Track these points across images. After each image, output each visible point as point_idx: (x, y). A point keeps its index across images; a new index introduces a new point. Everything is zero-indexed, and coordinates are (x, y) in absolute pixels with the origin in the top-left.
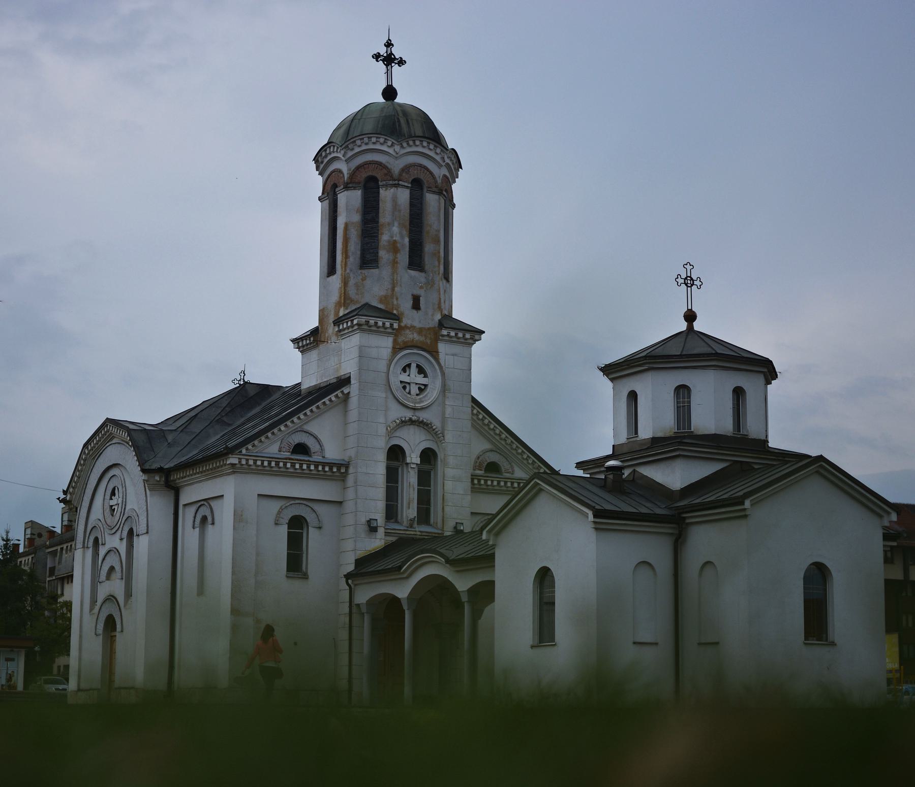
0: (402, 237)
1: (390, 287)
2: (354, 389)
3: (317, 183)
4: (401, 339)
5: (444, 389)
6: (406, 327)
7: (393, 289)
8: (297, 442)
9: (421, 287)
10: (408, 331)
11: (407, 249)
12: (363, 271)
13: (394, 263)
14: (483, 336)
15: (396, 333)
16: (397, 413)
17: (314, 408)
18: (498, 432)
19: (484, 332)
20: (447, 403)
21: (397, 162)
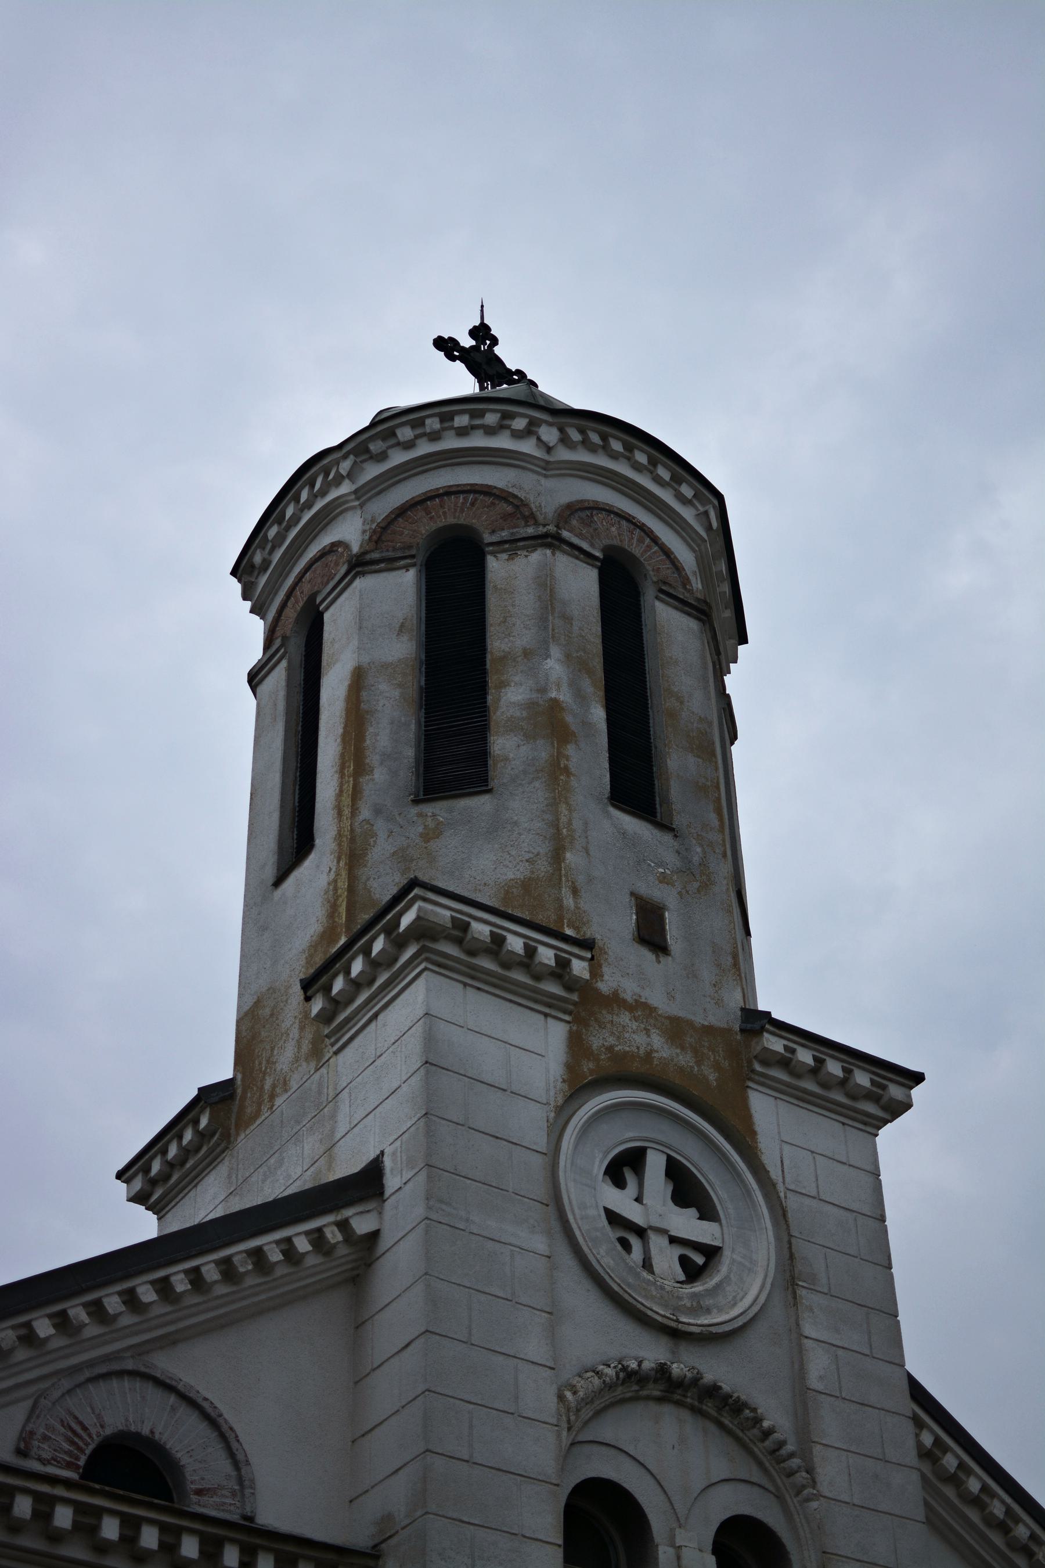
0: (579, 695)
1: (544, 848)
2: (399, 1216)
3: (249, 635)
4: (598, 1040)
5: (790, 1276)
6: (615, 1001)
7: (557, 856)
8: (114, 1422)
9: (663, 879)
10: (625, 1018)
11: (603, 740)
12: (428, 809)
13: (557, 773)
14: (917, 1093)
15: (582, 1005)
16: (602, 1340)
17: (209, 1266)
18: (998, 1510)
19: (918, 1078)
20: (808, 1330)
21: (547, 483)
